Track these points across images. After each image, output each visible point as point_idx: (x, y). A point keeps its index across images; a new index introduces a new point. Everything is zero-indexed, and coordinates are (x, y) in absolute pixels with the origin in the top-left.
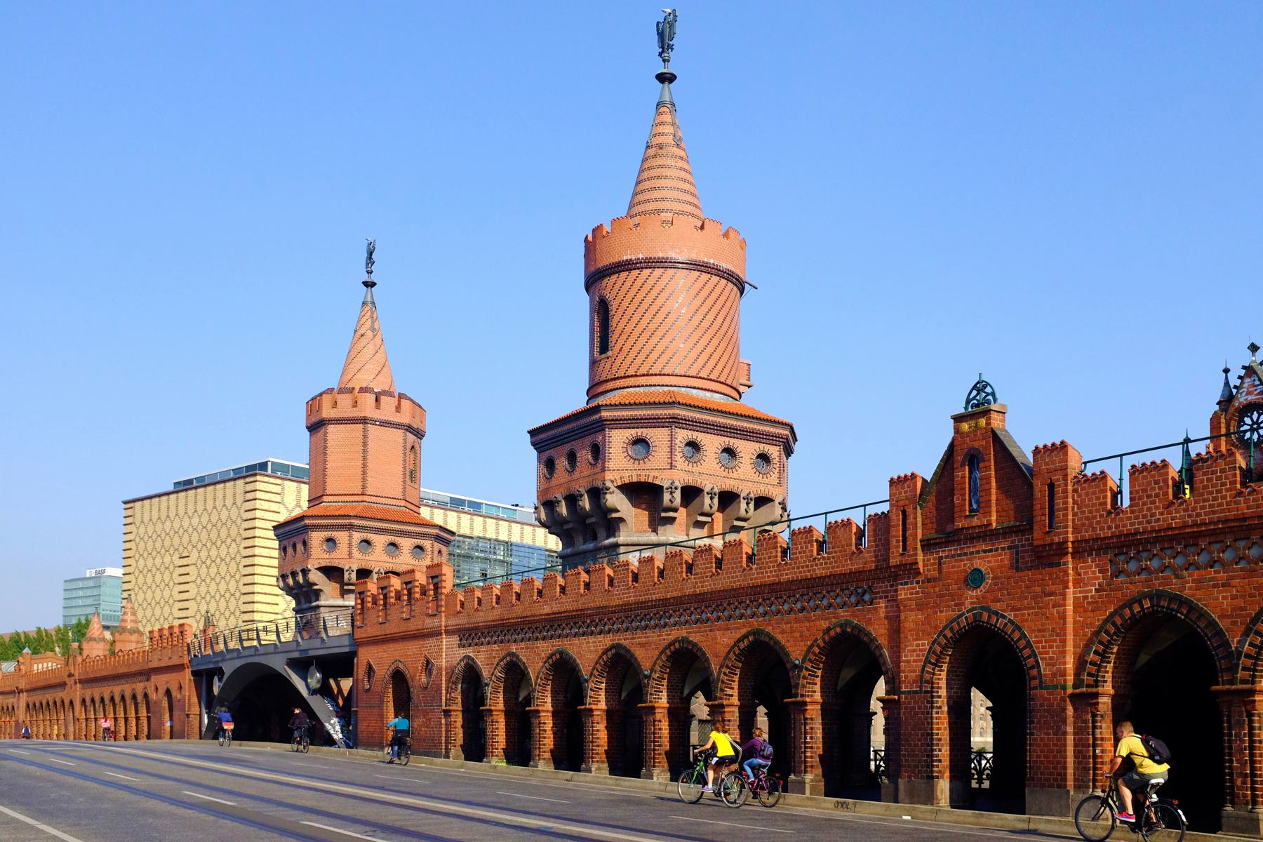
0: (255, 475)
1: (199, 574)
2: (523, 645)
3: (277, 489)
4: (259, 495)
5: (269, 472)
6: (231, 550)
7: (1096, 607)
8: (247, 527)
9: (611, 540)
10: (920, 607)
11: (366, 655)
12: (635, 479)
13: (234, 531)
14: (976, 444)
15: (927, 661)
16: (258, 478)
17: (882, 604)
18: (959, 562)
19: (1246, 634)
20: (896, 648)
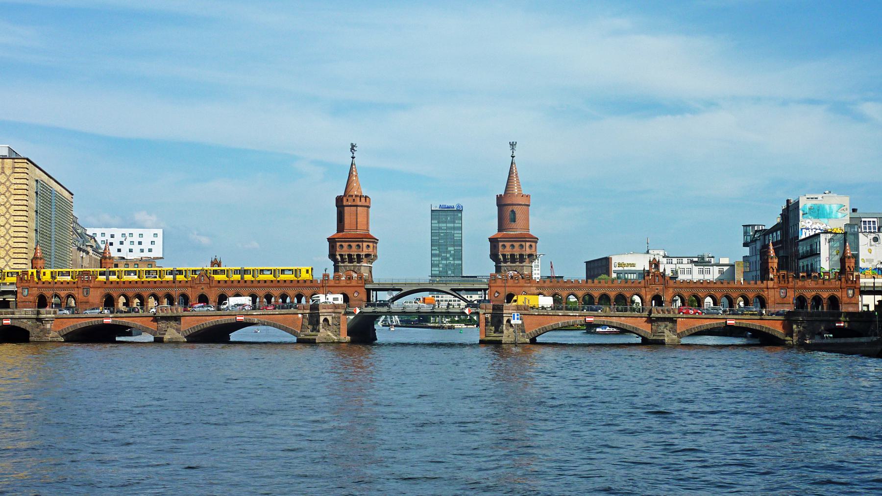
8: (16, 188)
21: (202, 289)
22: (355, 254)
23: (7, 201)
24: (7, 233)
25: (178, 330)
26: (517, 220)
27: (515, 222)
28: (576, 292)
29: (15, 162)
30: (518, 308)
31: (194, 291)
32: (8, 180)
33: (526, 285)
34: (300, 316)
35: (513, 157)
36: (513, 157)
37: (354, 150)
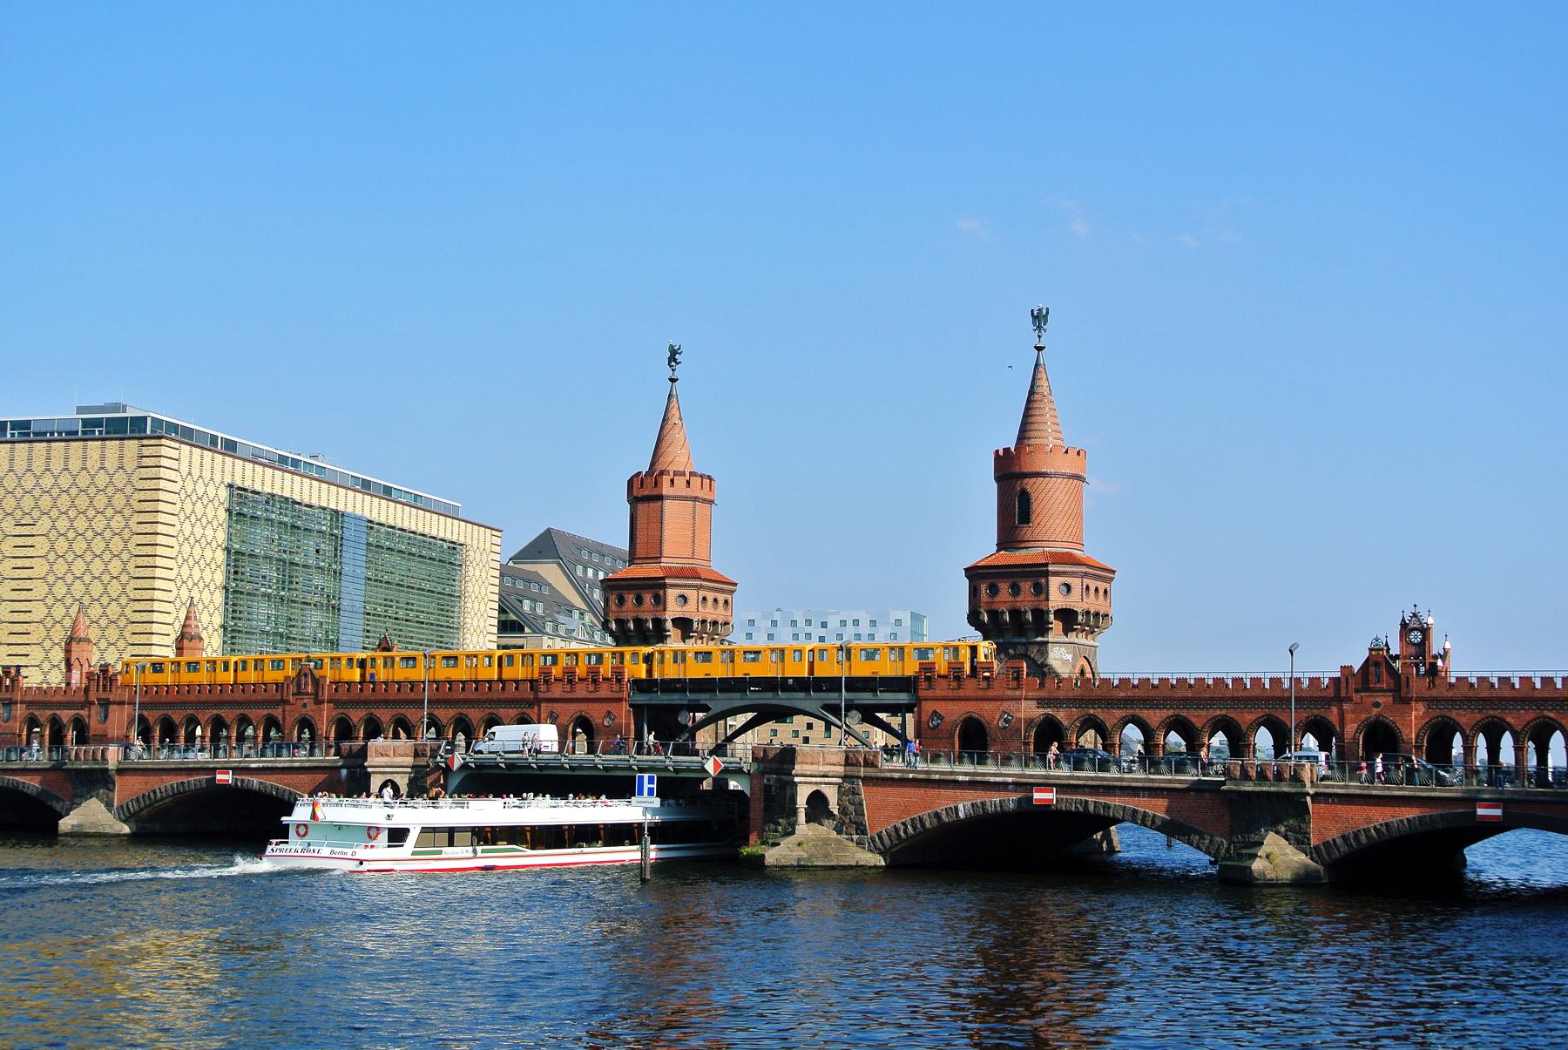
0: (160, 438)
1: (52, 548)
2: (1099, 710)
3: (174, 454)
4: (164, 462)
5: (148, 432)
6: (113, 524)
7: (1422, 718)
9: (1040, 639)
10: (1353, 712)
11: (928, 707)
12: (1064, 607)
13: (119, 501)
14: (1378, 660)
15: (1357, 732)
16: (163, 441)
17: (1335, 710)
18: (1370, 698)
19: (1471, 730)
20: (1342, 725)
21: (305, 705)
22: (650, 617)
23: (127, 526)
24: (124, 591)
25: (109, 805)
26: (1033, 517)
27: (1028, 522)
28: (1145, 714)
29: (143, 446)
30: (847, 757)
31: (290, 711)
32: (129, 482)
33: (1009, 693)
34: (344, 772)
35: (1039, 349)
36: (1039, 349)
37: (675, 360)
